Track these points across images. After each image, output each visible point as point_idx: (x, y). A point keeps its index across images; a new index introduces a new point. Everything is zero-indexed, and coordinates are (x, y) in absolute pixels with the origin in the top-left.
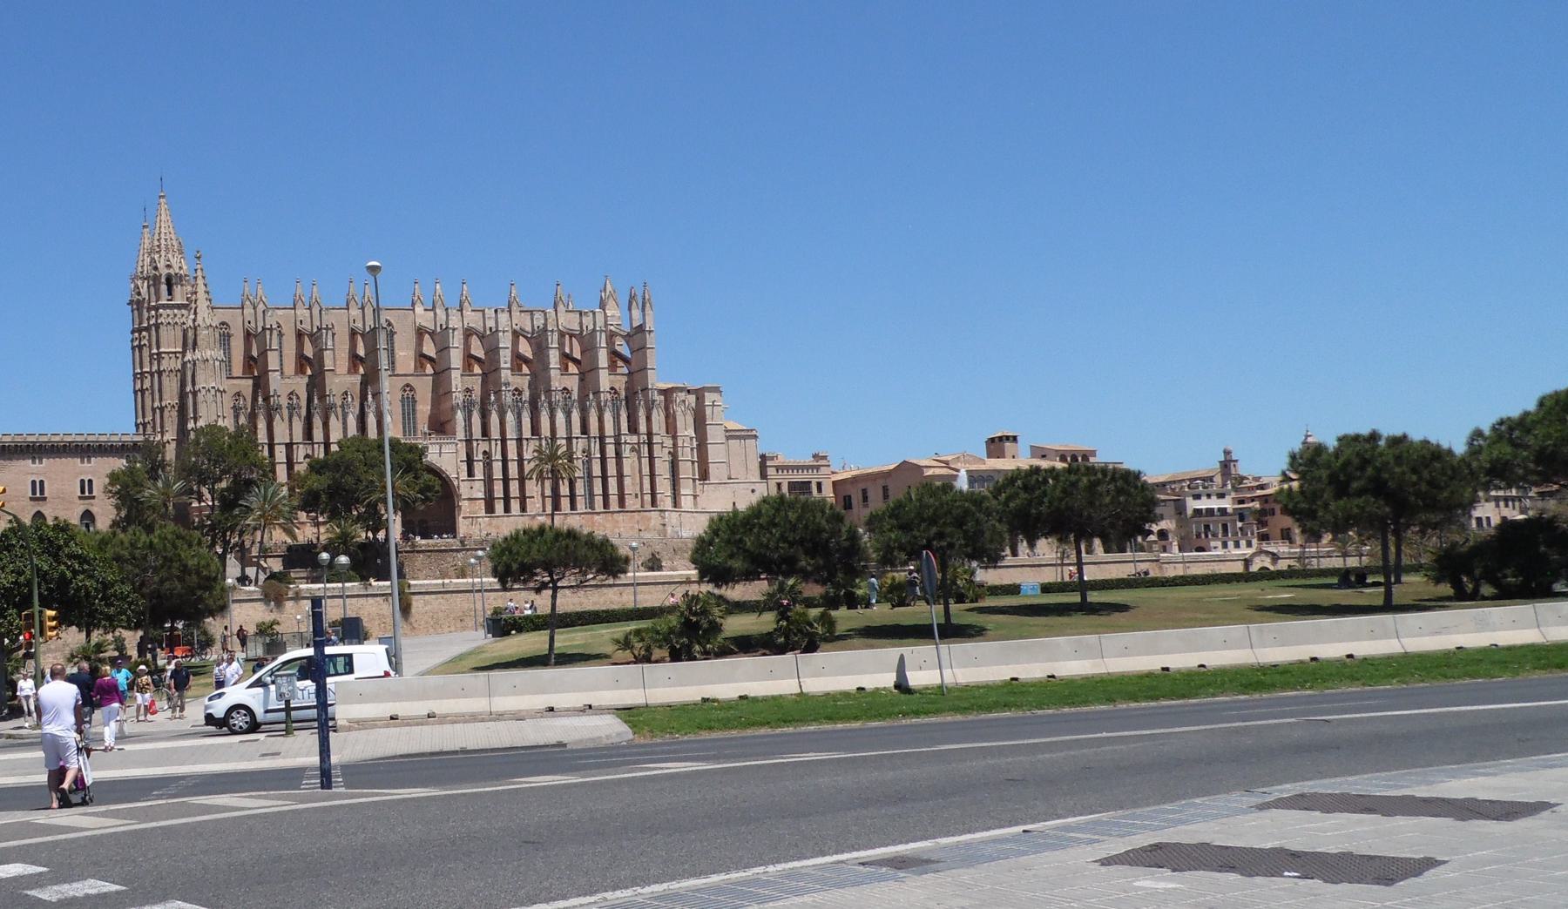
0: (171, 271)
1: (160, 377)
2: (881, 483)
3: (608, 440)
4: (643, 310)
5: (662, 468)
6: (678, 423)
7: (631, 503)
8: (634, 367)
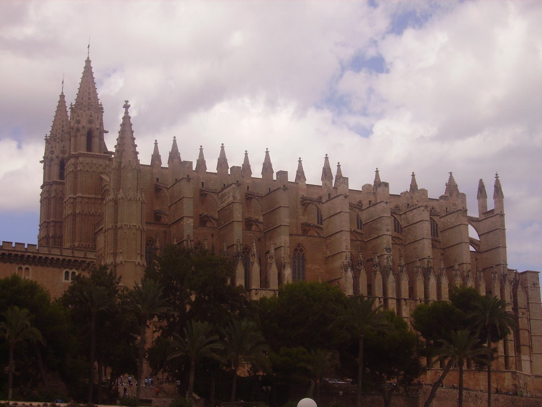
1: (74, 220)
6: (518, 298)
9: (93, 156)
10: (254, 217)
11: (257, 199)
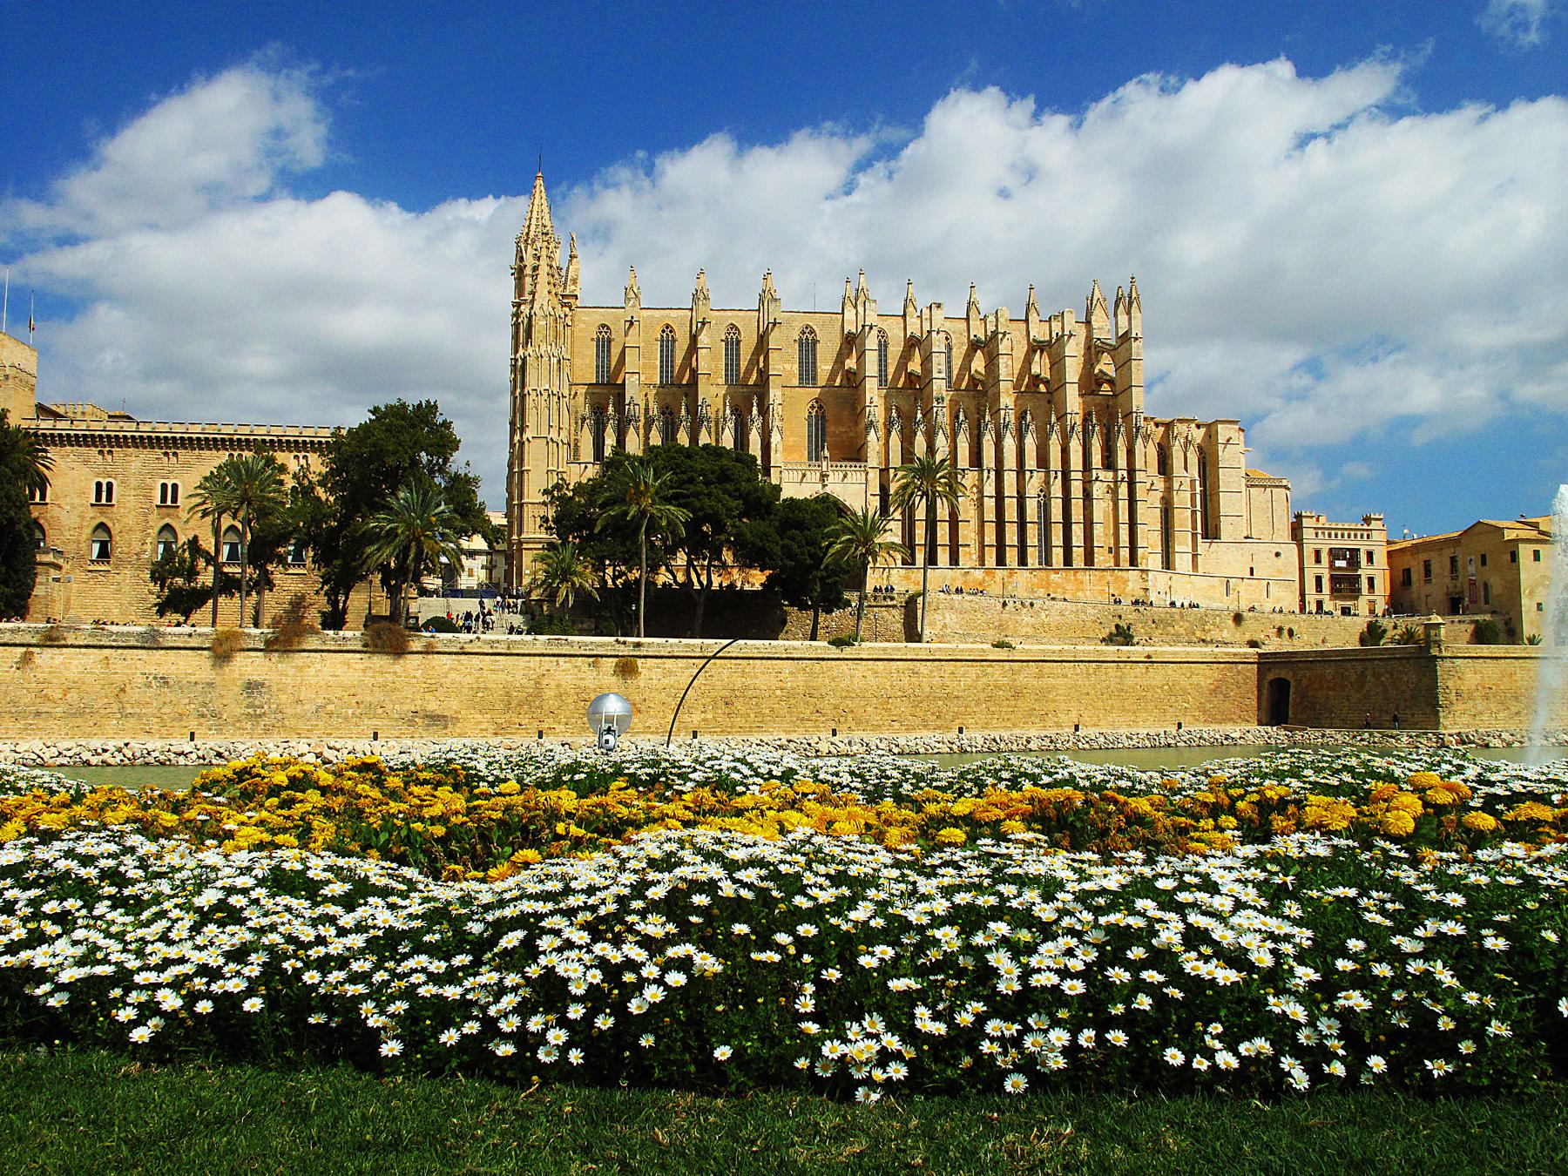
2: (1448, 553)
3: (1073, 475)
4: (1129, 313)
5: (1149, 516)
7: (1102, 558)
8: (1119, 388)
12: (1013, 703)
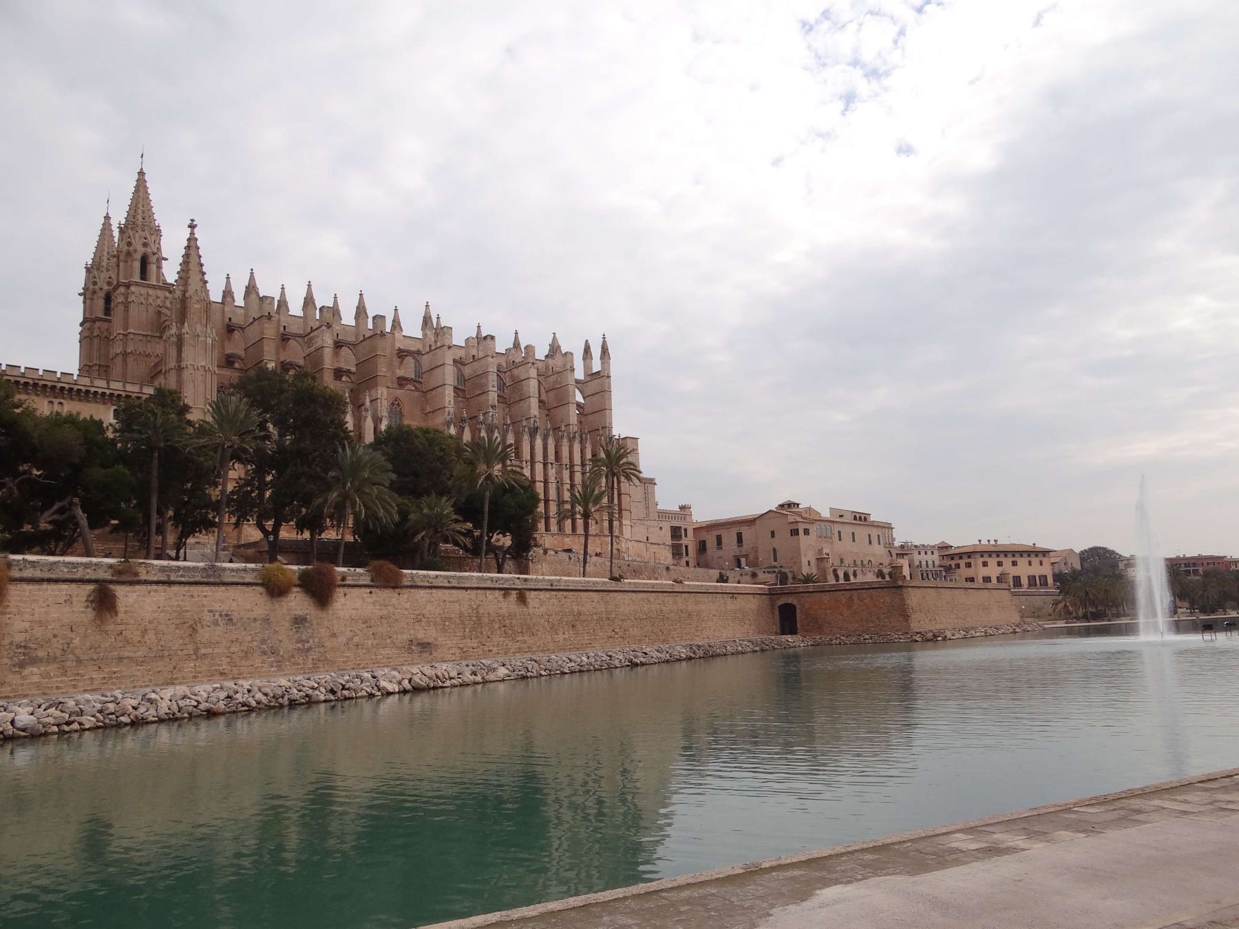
0: (149, 250)
1: (125, 360)
2: (734, 531)
9: (148, 286)
10: (345, 367)
11: (349, 348)
12: (689, 621)
